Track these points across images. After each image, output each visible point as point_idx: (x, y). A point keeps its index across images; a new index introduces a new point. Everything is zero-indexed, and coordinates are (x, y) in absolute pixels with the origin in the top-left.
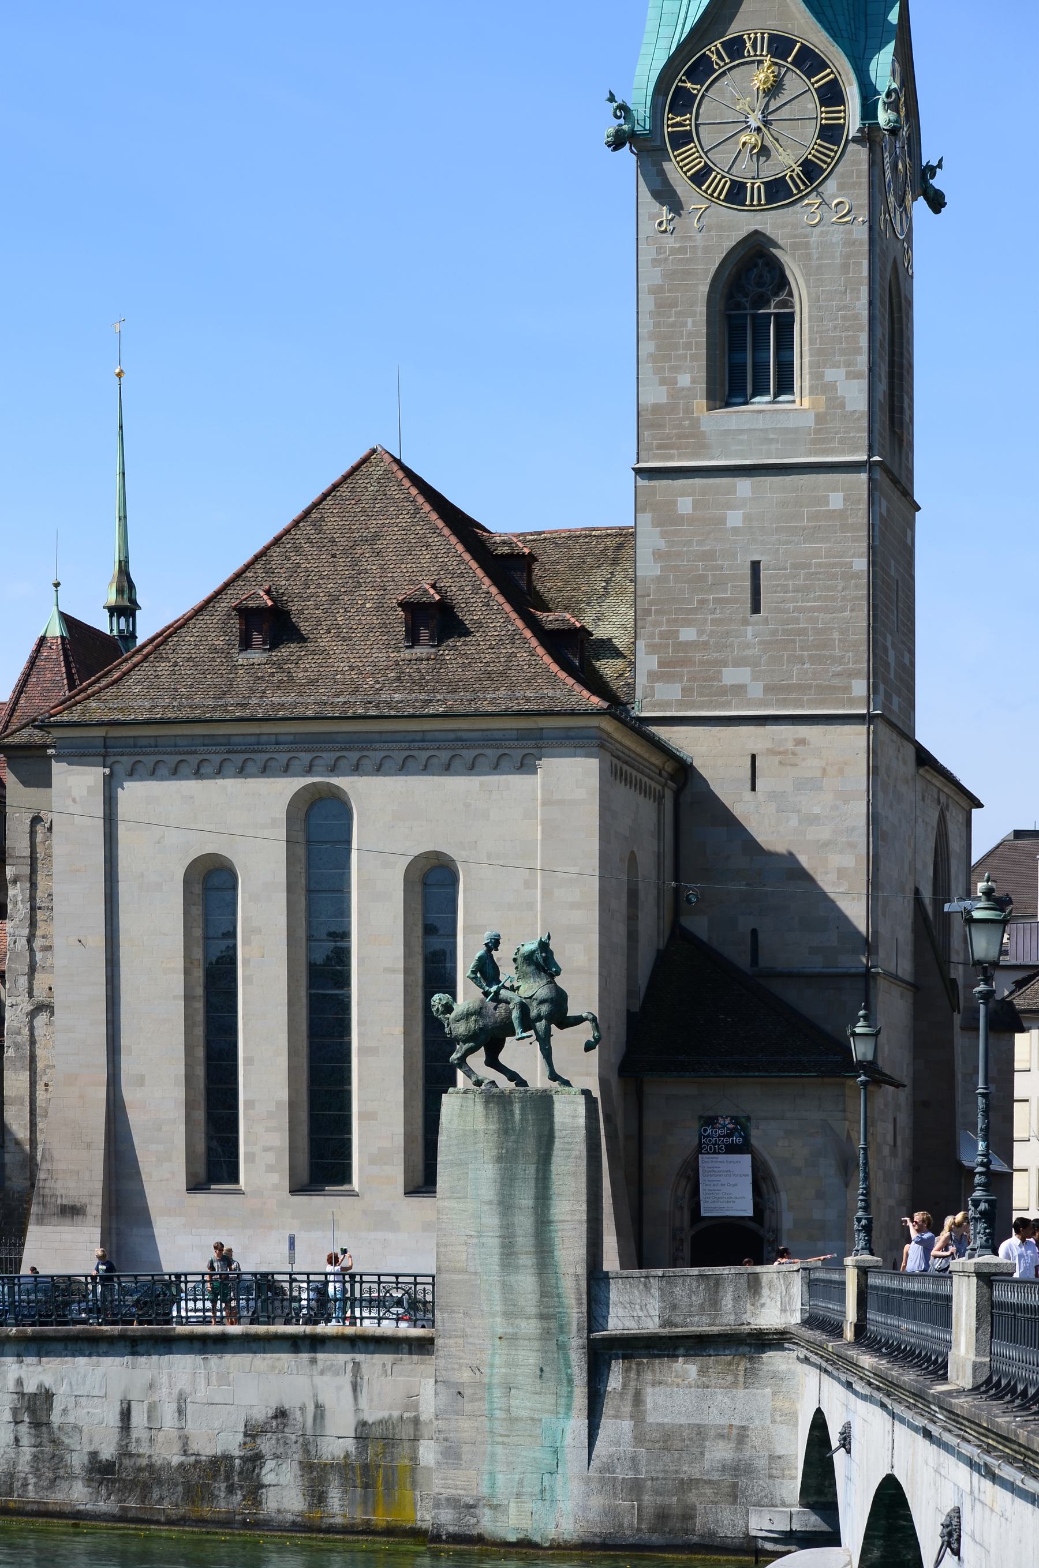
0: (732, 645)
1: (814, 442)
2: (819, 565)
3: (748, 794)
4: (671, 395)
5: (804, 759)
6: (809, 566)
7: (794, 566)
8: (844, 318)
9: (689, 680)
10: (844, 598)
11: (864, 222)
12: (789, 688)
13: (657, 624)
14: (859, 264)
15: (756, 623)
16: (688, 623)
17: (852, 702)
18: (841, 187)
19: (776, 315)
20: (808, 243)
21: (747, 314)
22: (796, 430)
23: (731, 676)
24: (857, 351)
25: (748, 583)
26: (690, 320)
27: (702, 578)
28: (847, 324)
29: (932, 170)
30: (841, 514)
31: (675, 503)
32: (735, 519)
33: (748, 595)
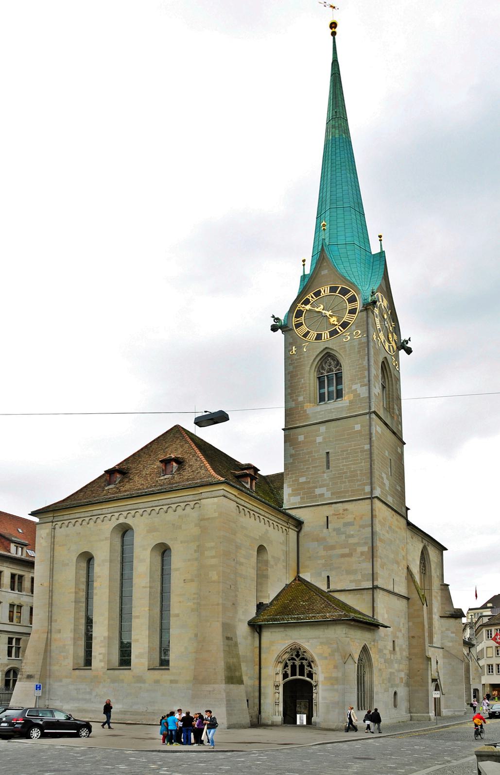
0: (318, 481)
2: (350, 450)
3: (325, 530)
5: (347, 516)
6: (347, 450)
7: (341, 451)
8: (359, 368)
11: (366, 336)
12: (341, 492)
15: (328, 472)
17: (365, 494)
18: (356, 327)
19: (335, 374)
20: (345, 347)
21: (324, 376)
23: (318, 491)
25: (325, 460)
28: (360, 369)
30: (359, 432)
32: (319, 439)
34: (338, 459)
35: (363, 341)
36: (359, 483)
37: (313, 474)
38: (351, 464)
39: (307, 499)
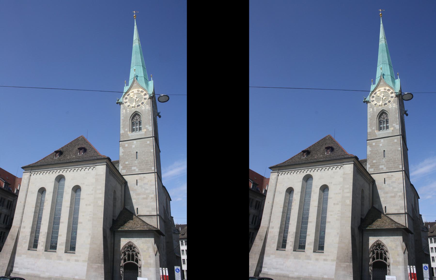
0: (381, 162)
1: (392, 133)
4: (372, 130)
7: (390, 150)
9: (375, 168)
10: (397, 154)
13: (370, 160)
14: (397, 111)
16: (374, 160)
17: (400, 169)
22: (389, 132)
24: (397, 121)
26: (374, 121)
27: (376, 153)
29: (406, 111)
31: (372, 144)
33: (383, 155)
34: (388, 153)
35: (396, 108)
36: (397, 164)
37: (379, 159)
38: (394, 156)
39: (376, 170)
